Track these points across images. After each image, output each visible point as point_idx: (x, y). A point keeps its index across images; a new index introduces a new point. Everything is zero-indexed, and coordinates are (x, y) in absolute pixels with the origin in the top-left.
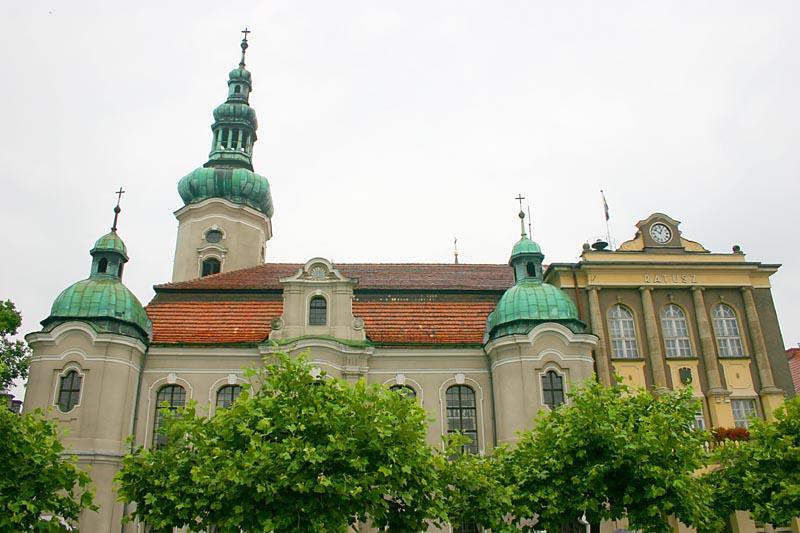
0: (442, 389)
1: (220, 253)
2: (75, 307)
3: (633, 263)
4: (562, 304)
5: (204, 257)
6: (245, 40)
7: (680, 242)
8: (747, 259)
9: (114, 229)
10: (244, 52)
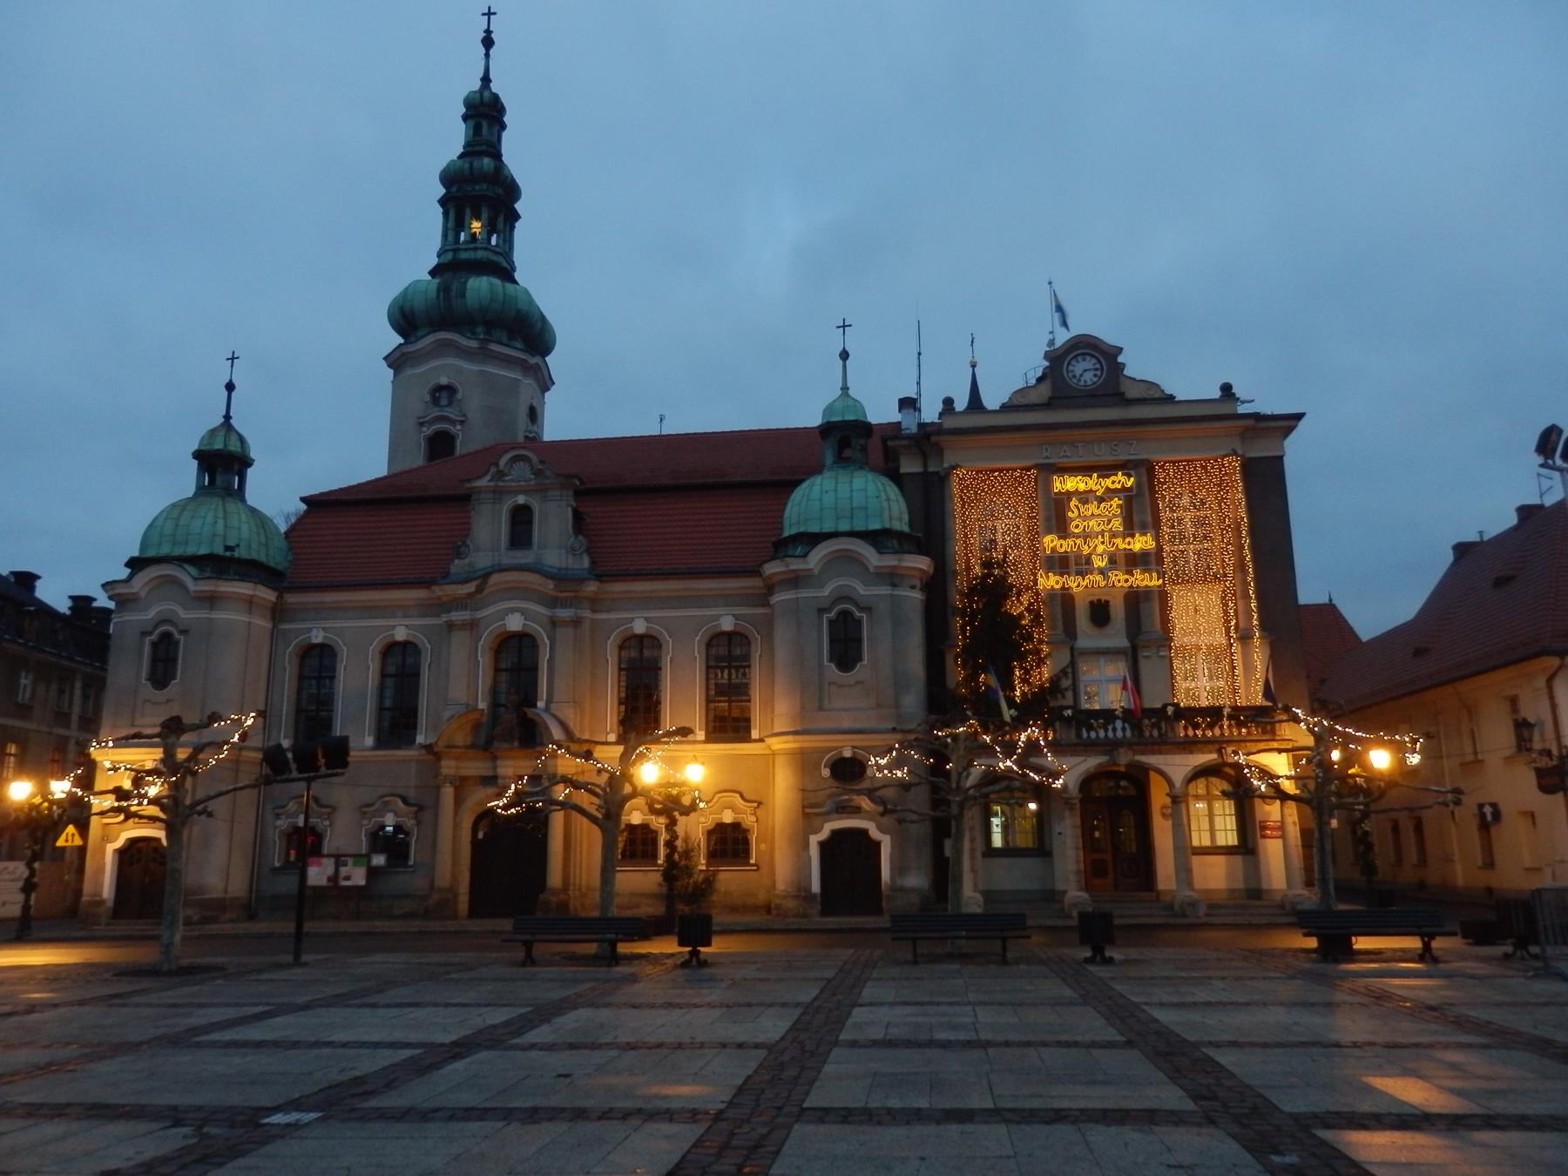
1: (453, 422)
5: (428, 431)
10: (487, 55)
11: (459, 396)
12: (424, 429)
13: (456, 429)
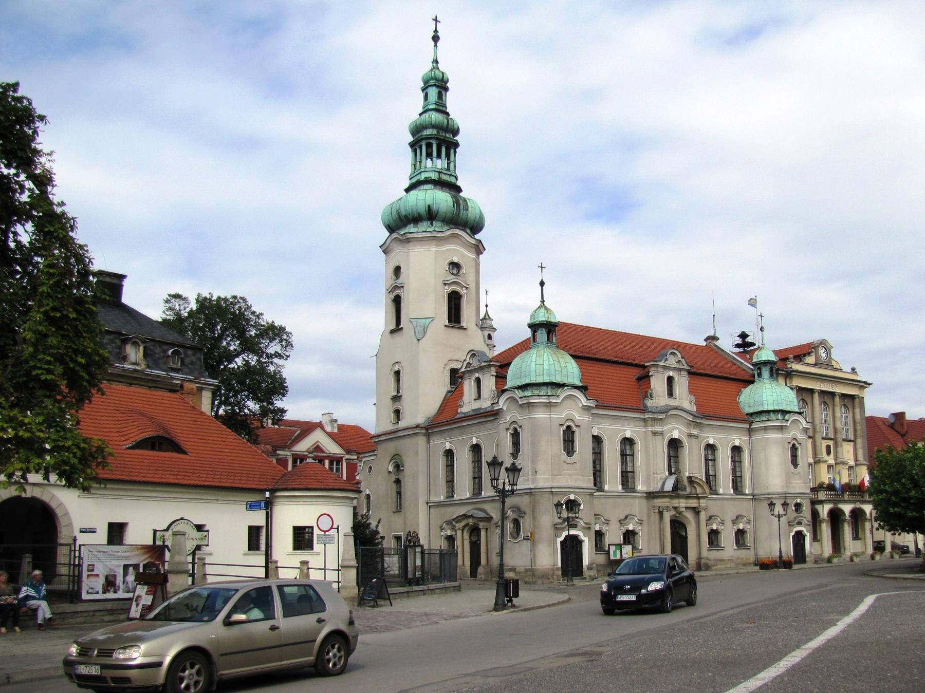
0: (729, 448)
2: (559, 374)
3: (810, 373)
4: (795, 401)
5: (450, 289)
6: (436, 31)
7: (831, 363)
8: (859, 378)
9: (543, 302)
11: (463, 271)
12: (446, 287)
13: (462, 291)
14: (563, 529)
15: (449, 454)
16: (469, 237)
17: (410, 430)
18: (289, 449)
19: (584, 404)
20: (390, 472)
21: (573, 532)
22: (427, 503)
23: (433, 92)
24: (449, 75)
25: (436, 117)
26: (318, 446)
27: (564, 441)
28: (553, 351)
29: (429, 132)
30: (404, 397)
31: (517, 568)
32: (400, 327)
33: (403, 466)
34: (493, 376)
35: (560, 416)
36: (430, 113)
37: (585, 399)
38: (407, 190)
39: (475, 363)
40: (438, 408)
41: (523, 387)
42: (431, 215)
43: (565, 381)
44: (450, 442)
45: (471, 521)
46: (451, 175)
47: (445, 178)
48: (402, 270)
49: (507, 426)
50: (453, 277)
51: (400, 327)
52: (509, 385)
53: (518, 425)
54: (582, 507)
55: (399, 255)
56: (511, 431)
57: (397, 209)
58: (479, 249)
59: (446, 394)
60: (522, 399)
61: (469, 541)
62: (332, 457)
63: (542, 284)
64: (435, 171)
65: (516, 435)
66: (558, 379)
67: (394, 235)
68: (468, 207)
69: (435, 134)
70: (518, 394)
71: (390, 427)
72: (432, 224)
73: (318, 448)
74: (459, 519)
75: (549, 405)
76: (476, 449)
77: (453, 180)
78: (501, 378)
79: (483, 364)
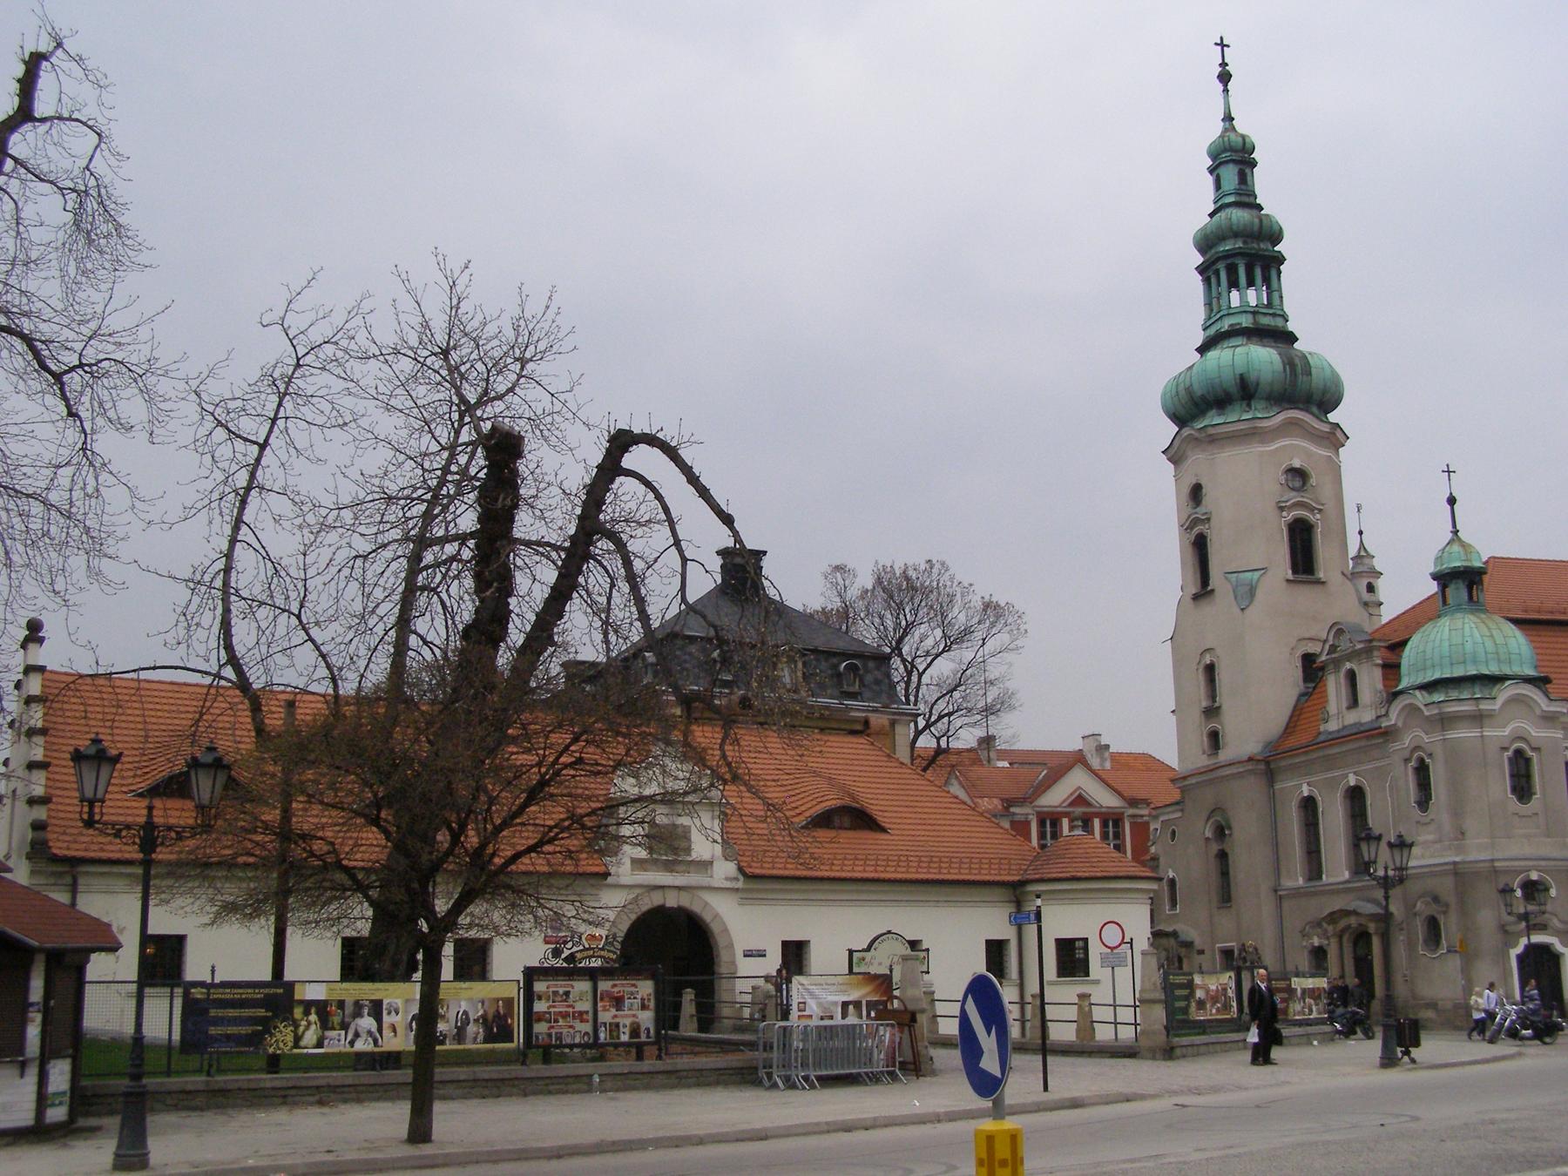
1: (1312, 510)
5: (1290, 516)
9: (1455, 532)
10: (1226, 91)
11: (1313, 481)
12: (1284, 514)
13: (1313, 518)
14: (1520, 935)
15: (1309, 805)
16: (1317, 421)
17: (1237, 765)
18: (1031, 803)
19: (1545, 709)
20: (1207, 839)
21: (1537, 938)
22: (1276, 891)
23: (1230, 175)
24: (1255, 138)
25: (1239, 216)
26: (1080, 796)
27: (1512, 776)
28: (1481, 619)
29: (1227, 246)
30: (1224, 708)
31: (1440, 1003)
32: (1209, 588)
33: (1230, 828)
34: (1377, 665)
35: (1501, 732)
36: (1229, 211)
37: (1546, 700)
38: (1202, 350)
39: (1344, 645)
40: (1284, 724)
41: (1430, 687)
42: (1245, 391)
43: (1507, 671)
44: (1308, 784)
45: (1353, 921)
46: (1274, 315)
47: (1265, 321)
48: (1204, 490)
49: (1406, 754)
50: (1293, 494)
51: (1209, 588)
52: (1403, 684)
53: (1424, 751)
54: (1553, 892)
55: (1200, 463)
56: (1413, 763)
57: (1188, 384)
58: (1335, 438)
59: (1298, 700)
60: (1431, 707)
61: (1352, 955)
62: (1105, 813)
63: (1452, 501)
64: (1245, 312)
65: (1422, 771)
66: (1493, 669)
67: (1186, 431)
68: (1310, 367)
69: (1240, 248)
70: (1420, 698)
71: (1203, 761)
72: (1249, 405)
73: (1080, 800)
74: (1333, 917)
75: (1479, 718)
76: (1356, 796)
77: (1279, 322)
78: (1391, 669)
79: (1359, 646)
